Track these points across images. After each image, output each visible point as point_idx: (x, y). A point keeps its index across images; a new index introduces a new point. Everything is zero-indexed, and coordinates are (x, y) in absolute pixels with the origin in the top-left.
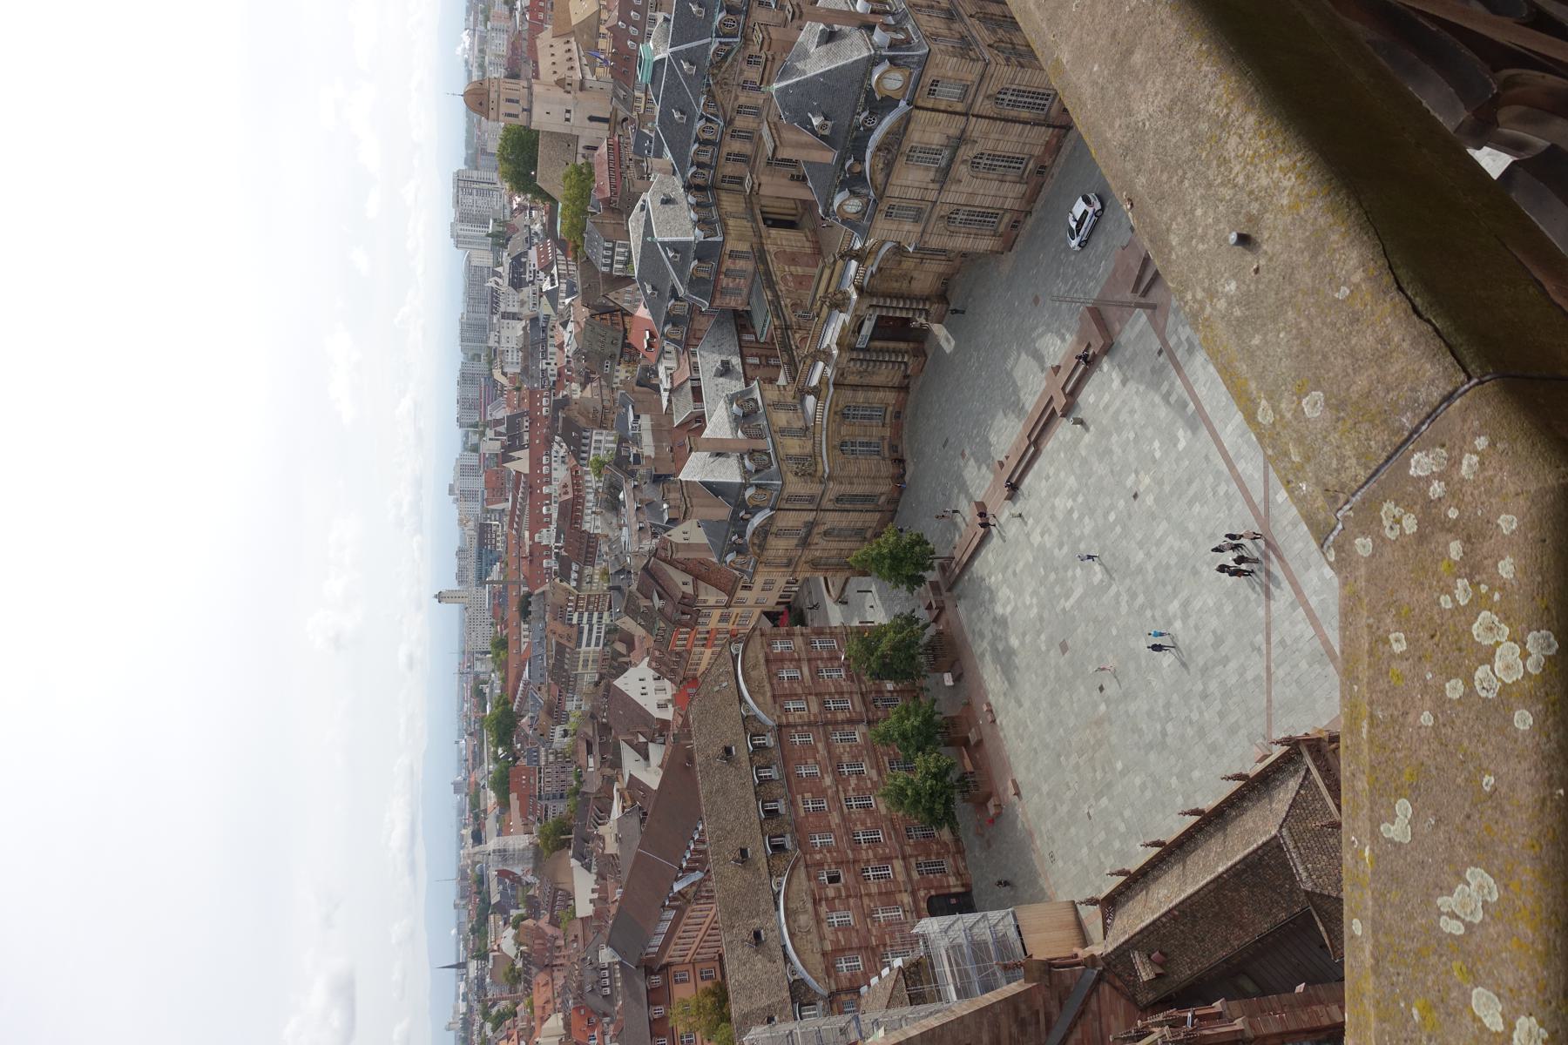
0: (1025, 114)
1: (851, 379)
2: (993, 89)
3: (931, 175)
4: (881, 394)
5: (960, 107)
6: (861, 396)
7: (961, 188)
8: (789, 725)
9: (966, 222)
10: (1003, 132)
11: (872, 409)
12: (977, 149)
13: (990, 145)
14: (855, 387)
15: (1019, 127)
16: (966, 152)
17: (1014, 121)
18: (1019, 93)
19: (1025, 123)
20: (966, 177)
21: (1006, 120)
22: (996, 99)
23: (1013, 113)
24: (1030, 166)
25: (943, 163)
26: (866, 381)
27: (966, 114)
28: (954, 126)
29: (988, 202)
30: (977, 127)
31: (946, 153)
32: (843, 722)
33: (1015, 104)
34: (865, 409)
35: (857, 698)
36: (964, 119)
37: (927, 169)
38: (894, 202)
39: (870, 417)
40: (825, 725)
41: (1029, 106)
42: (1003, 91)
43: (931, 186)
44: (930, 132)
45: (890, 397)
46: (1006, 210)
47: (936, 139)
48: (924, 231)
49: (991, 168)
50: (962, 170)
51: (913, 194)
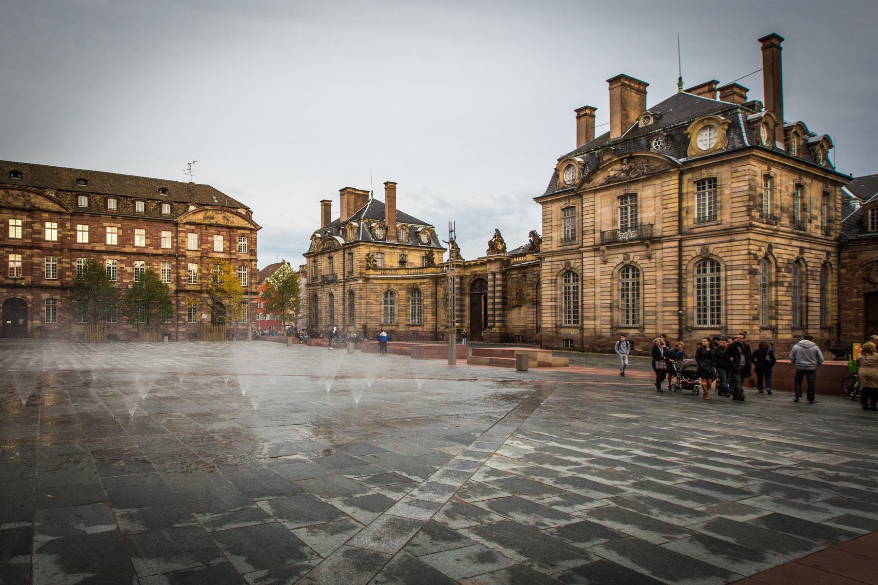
0: (691, 302)
1: (441, 291)
2: (717, 248)
3: (607, 228)
4: (430, 317)
5: (688, 223)
6: (427, 302)
7: (598, 267)
8: (178, 232)
9: (567, 294)
10: (666, 282)
11: (419, 315)
12: (643, 264)
13: (648, 275)
14: (435, 295)
15: (673, 297)
16: (636, 255)
17: (681, 290)
18: (716, 283)
19: (680, 304)
20: (609, 267)
21: (680, 280)
22: (707, 260)
23: (690, 287)
24: (633, 332)
25: (621, 236)
26: (440, 304)
27: (680, 232)
28: (664, 226)
29: (588, 301)
30: (667, 252)
31: (631, 234)
32: (178, 273)
33: (701, 286)
34: (420, 309)
35: (198, 288)
36: (677, 232)
37: (614, 222)
38: (578, 209)
39: (413, 315)
40: (177, 256)
41: (701, 307)
42: (716, 265)
43: (598, 235)
44: (655, 202)
45: (428, 326)
46: (582, 328)
47: (647, 215)
48: (552, 254)
49: (624, 291)
50: (617, 258)
51: (588, 221)
